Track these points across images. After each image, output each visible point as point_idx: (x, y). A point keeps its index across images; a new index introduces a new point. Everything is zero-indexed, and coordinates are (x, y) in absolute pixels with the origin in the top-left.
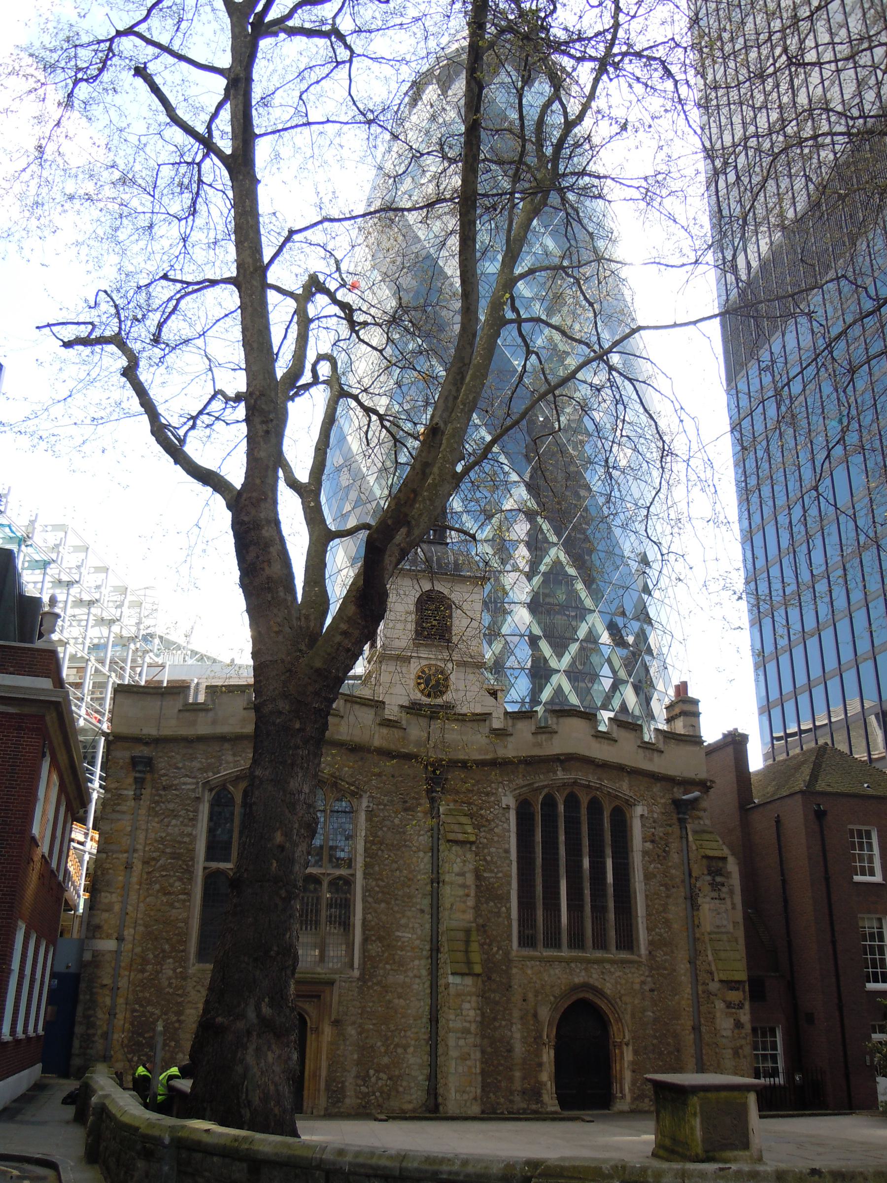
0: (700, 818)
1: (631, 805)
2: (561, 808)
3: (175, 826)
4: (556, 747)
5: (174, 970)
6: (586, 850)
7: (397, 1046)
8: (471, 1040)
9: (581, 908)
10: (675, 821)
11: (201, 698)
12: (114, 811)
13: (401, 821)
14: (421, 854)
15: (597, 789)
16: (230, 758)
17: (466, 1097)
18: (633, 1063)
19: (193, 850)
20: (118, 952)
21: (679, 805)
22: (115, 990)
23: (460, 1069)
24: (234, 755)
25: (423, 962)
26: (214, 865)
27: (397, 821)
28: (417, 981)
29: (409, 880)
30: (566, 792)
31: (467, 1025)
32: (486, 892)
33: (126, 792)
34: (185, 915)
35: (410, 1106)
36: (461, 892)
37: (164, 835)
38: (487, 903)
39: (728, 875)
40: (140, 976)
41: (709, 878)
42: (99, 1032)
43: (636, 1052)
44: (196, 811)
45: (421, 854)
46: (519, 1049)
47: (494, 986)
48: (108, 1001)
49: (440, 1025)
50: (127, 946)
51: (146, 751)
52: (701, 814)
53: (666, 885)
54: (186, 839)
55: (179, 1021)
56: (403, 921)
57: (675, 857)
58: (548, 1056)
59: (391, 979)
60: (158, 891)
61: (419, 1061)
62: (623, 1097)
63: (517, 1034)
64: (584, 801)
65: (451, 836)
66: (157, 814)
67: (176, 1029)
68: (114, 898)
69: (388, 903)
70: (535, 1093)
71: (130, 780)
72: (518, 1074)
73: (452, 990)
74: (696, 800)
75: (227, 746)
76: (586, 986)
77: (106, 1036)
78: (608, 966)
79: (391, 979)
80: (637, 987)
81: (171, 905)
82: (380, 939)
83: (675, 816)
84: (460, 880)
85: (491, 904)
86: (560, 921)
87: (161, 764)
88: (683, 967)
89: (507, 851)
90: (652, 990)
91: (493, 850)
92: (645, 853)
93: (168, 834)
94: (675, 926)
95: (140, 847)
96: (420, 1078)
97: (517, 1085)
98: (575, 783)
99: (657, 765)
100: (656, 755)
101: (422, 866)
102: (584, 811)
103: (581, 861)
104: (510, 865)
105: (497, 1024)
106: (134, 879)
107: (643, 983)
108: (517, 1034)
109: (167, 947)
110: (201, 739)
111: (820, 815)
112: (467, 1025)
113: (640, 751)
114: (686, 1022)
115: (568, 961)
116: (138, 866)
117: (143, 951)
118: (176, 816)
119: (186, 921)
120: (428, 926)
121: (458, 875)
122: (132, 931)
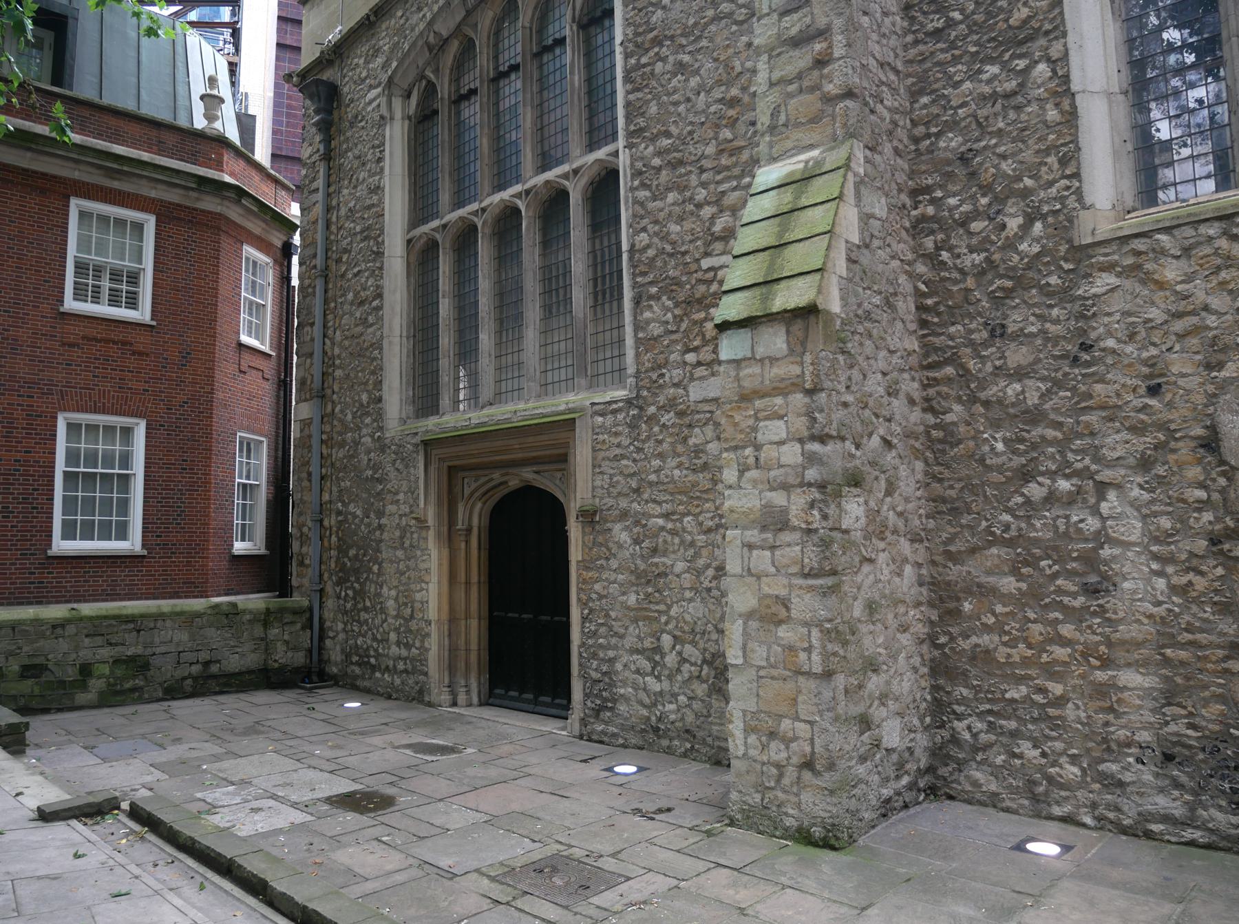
17: (777, 752)
23: (759, 654)
29: (733, 102)
31: (779, 498)
36: (800, 60)
38: (974, 76)
55: (380, 527)
69: (682, 189)
79: (696, 392)
82: (670, 287)
85: (994, 69)
105: (1035, 491)
112: (779, 498)
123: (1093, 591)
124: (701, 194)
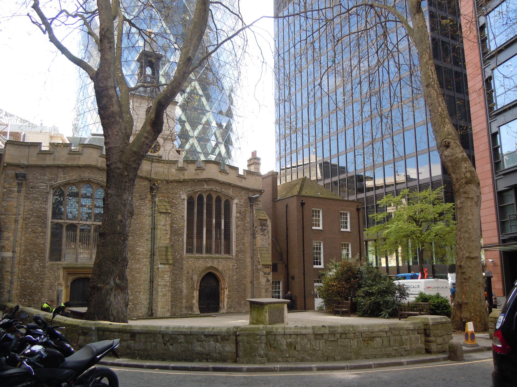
0: (258, 204)
1: (232, 199)
2: (205, 200)
3: (38, 204)
4: (204, 175)
5: (39, 264)
6: (214, 216)
7: (136, 292)
8: (167, 289)
9: (211, 238)
10: (249, 205)
11: (47, 149)
12: (8, 197)
13: (139, 204)
14: (147, 217)
15: (220, 193)
16: (62, 176)
17: (165, 310)
18: (228, 295)
19: (46, 214)
20: (13, 258)
21: (250, 199)
22: (12, 273)
23: (163, 300)
24: (64, 174)
25: (148, 260)
26: (56, 221)
27: (137, 204)
28: (145, 267)
30: (207, 194)
32: (175, 232)
33: (13, 189)
34: (43, 242)
35: (141, 315)
37: (32, 208)
39: (267, 226)
40: (24, 267)
41: (260, 227)
42: (6, 290)
43: (229, 291)
44: (47, 198)
45: (147, 217)
46: (185, 292)
47: (176, 268)
48: (9, 277)
49: (154, 283)
50: (17, 255)
51: (22, 171)
52: (259, 203)
53: (244, 230)
54: (43, 210)
55: (42, 285)
56: (139, 244)
57: (248, 219)
58: (196, 294)
59: (134, 266)
60: (31, 232)
61: (145, 297)
62: (224, 308)
63: (184, 286)
64: (214, 197)
65: (160, 211)
66: (29, 199)
67: (40, 288)
68: (10, 234)
69: (133, 237)
70: (191, 308)
71: (15, 184)
72: (184, 301)
73: (160, 270)
74: (257, 197)
75: (60, 170)
76: (212, 267)
77: (9, 292)
78: (220, 260)
79: (134, 266)
80: (231, 267)
81: (37, 238)
83: (249, 204)
84: (164, 228)
86: (202, 243)
87: (30, 177)
88: (248, 260)
89: (183, 216)
90: (236, 268)
91: (177, 216)
92: (237, 217)
93: (34, 208)
94: (246, 245)
95: (21, 213)
96: (146, 304)
97: (184, 305)
98: (211, 190)
99: (243, 184)
100: (243, 180)
101: (147, 222)
102: (214, 201)
103: (212, 221)
104: (184, 222)
105: (177, 282)
106: (19, 227)
107: (233, 266)
108: (184, 286)
109: (36, 255)
110: (48, 167)
111: (303, 204)
113: (237, 178)
114: (249, 280)
115: (205, 258)
116: (21, 221)
117: (25, 257)
118: (38, 200)
119: (44, 244)
120: (150, 246)
121: (163, 226)
122: (19, 248)
123: (181, 292)
124: (136, 239)
